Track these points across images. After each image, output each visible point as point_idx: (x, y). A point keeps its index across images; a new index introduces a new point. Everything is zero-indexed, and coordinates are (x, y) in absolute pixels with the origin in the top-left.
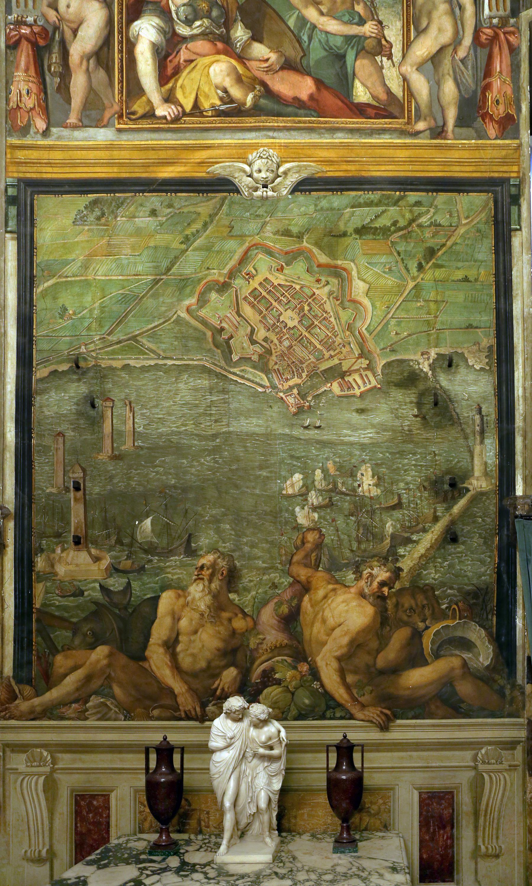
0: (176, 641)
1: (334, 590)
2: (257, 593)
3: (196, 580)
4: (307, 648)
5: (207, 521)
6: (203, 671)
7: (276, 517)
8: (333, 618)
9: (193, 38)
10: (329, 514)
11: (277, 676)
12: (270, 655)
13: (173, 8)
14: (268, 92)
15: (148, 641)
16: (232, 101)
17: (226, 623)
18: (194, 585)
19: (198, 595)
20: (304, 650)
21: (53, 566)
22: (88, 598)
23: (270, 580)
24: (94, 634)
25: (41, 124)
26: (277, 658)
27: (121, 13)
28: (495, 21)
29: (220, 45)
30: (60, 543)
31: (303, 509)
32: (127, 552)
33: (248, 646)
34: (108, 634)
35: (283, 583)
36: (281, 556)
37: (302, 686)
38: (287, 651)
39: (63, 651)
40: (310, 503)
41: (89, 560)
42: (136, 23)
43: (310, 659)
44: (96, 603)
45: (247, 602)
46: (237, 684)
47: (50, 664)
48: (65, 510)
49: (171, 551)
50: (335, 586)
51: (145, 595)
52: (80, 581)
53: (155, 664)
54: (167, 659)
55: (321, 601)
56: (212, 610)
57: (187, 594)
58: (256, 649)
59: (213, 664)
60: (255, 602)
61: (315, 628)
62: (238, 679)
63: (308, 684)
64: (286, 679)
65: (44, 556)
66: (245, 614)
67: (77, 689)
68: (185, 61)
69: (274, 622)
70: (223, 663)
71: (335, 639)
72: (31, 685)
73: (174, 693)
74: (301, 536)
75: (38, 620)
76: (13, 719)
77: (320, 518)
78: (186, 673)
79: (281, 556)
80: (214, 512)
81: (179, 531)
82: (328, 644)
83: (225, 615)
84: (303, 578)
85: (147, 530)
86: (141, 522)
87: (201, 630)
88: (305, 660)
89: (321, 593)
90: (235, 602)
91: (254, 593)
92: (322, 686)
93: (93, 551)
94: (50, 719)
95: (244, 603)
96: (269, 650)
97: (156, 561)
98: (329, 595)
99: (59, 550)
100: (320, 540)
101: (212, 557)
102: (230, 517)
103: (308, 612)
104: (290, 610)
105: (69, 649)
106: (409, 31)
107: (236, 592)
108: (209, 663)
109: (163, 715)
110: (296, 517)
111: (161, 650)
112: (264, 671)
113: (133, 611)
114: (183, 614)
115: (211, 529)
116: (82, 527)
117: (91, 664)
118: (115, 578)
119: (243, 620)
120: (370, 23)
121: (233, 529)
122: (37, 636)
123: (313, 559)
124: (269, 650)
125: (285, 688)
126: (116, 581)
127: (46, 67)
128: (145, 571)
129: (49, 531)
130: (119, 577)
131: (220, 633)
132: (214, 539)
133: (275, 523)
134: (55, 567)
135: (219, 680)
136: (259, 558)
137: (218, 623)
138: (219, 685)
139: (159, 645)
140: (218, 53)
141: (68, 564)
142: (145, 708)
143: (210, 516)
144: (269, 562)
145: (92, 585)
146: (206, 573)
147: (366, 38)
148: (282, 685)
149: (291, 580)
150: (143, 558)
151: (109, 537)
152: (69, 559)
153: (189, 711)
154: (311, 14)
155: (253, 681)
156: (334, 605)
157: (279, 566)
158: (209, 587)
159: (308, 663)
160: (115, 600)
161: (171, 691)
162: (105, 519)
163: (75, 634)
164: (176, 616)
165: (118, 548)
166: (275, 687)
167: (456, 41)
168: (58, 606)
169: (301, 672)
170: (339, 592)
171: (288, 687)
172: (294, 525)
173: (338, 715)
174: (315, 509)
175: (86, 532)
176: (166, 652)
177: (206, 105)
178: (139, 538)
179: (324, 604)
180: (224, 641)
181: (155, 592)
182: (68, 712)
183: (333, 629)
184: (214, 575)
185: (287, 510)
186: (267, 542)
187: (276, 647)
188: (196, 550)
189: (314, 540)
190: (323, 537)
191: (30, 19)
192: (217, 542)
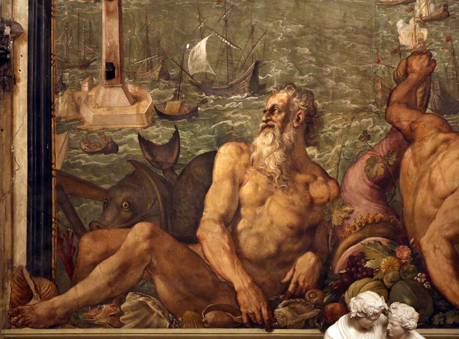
0: (238, 216)
1: (446, 141)
2: (343, 146)
3: (263, 128)
4: (408, 225)
5: (280, 42)
6: (272, 257)
7: (370, 36)
8: (444, 181)
10: (443, 29)
11: (368, 264)
12: (359, 235)
15: (201, 216)
17: (301, 188)
18: (262, 134)
19: (266, 150)
20: (405, 228)
21: (77, 109)
22: (124, 155)
23: (361, 127)
24: (131, 206)
26: (368, 239)
30: (87, 76)
31: (408, 23)
32: (174, 89)
33: (330, 221)
34: (149, 206)
35: (378, 131)
36: (376, 92)
37: (402, 279)
38: (381, 230)
39: (91, 230)
40: (417, 15)
41: (124, 100)
43: (412, 241)
44: (133, 162)
45: (330, 160)
46: (316, 277)
47: (75, 248)
48: (94, 28)
49: (232, 86)
50: (448, 136)
51: (198, 150)
52: (113, 131)
53: (209, 249)
54: (225, 241)
55: (429, 157)
56: (284, 170)
57: (251, 149)
58: (341, 227)
59: (284, 248)
60: (340, 160)
61: (419, 196)
62: (317, 268)
63: (409, 276)
64: (380, 268)
65: (66, 95)
66: (327, 177)
67: (110, 284)
69: (364, 187)
70: (296, 247)
71: (446, 212)
72: (51, 279)
73: (233, 288)
74: (403, 63)
75: (59, 187)
77: (430, 35)
78: (250, 261)
79: (376, 92)
80: (289, 30)
81: (243, 58)
82: (437, 219)
83: (301, 178)
84: (405, 124)
85: (201, 57)
86: (193, 44)
87: (269, 200)
88: (406, 242)
89: (428, 145)
90: (313, 160)
91: (339, 146)
92: (429, 278)
93: (131, 88)
94: (75, 326)
95: (326, 161)
96: (358, 228)
97: (212, 101)
98: (439, 149)
99: (86, 87)
100: (430, 69)
101: (285, 94)
102: (310, 37)
103: (410, 173)
104: (386, 171)
105: (98, 228)
107: (316, 145)
108: (279, 245)
109: (219, 320)
110: (398, 35)
111: (217, 228)
112: (351, 258)
113: (182, 174)
114: (247, 177)
115: (284, 55)
116: (115, 52)
117: (127, 248)
118: (158, 127)
119: (324, 186)
121: (313, 55)
122: (57, 211)
123: (419, 96)
124: (358, 228)
125: (379, 282)
126: (160, 130)
128: (197, 116)
129: (73, 58)
130: (164, 124)
131: (293, 203)
132: (289, 69)
133: (369, 45)
134: (81, 111)
135: (292, 271)
136: (346, 96)
137: (291, 190)
138: (292, 277)
139: (215, 221)
141: (98, 106)
142: (195, 311)
143: (283, 36)
144: (360, 100)
145: (129, 136)
146: (278, 117)
148: (375, 278)
149: (389, 127)
150: (195, 98)
151: (151, 68)
152: (99, 100)
153: (253, 313)
155: (336, 272)
156: (445, 162)
157: (374, 107)
158: (281, 138)
159: (410, 246)
160: (159, 158)
161: (229, 286)
162: (146, 41)
163: (106, 205)
164: (238, 181)
165: (163, 83)
166: (365, 280)
168: (84, 167)
169: (400, 259)
170: (453, 144)
171: (382, 281)
172: (395, 47)
173: (450, 321)
174: (423, 22)
175: (122, 60)
176: (224, 232)
178: (190, 68)
179: (432, 162)
180: (300, 215)
181: (210, 145)
182: (98, 316)
183: (444, 198)
184: (288, 121)
185: (386, 26)
186: (359, 72)
187: (367, 223)
188: (264, 86)
189: (421, 69)
190: (433, 64)
192: (292, 73)
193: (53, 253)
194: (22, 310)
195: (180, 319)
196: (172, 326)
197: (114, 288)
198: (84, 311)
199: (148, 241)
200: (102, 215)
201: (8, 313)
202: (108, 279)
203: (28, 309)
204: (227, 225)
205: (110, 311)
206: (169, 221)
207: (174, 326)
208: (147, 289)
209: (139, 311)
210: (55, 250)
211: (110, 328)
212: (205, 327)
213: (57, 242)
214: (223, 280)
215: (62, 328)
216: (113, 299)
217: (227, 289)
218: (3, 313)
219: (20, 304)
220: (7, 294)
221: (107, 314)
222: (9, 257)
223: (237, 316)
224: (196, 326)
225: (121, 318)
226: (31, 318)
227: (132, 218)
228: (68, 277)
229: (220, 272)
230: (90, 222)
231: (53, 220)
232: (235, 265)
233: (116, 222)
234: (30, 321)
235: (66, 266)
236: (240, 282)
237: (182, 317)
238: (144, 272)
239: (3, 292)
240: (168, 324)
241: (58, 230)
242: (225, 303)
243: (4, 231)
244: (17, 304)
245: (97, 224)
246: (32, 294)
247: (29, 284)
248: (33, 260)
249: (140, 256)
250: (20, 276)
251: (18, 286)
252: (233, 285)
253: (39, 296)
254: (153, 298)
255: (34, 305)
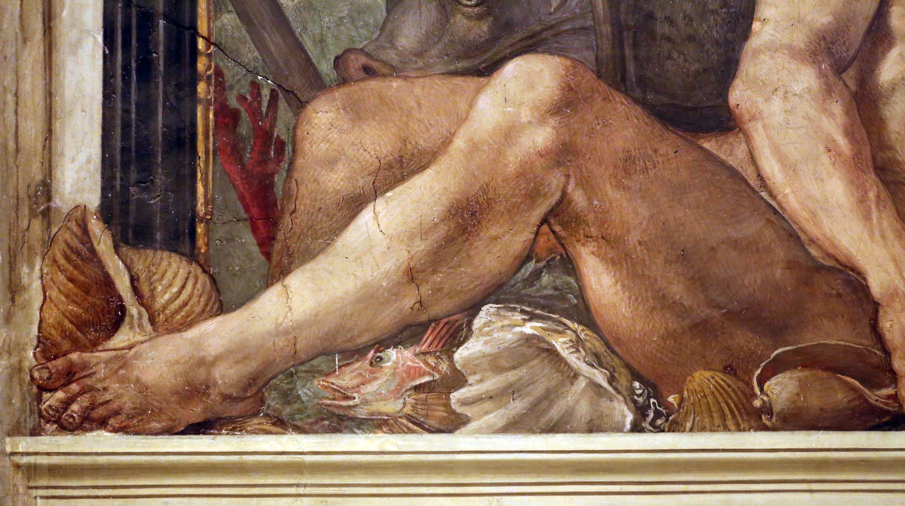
15: (746, 34)
39: (344, 81)
47: (281, 145)
53: (777, 151)
67: (412, 275)
72: (192, 256)
76: (102, 424)
94: (281, 424)
105: (369, 72)
109: (814, 401)
139: (795, 53)
142: (729, 369)
176: (828, 90)
193: (201, 163)
194: (85, 366)
195: (671, 399)
196: (646, 425)
197: (425, 290)
198: (314, 373)
199: (553, 121)
200: (382, 29)
201: (32, 378)
202: (404, 255)
203: (108, 362)
204: (840, 69)
205: (412, 373)
206: (628, 52)
207: (652, 424)
208: (550, 292)
209: (522, 372)
210: (207, 152)
211: (413, 432)
212: (765, 428)
213: (216, 122)
214: (830, 263)
215: (233, 431)
216: (425, 326)
217: (841, 291)
218: (11, 378)
219: (77, 346)
220: (25, 306)
221: (403, 380)
222: (36, 173)
223: (880, 386)
224: (730, 423)
225: (455, 396)
226: (119, 396)
227: (494, 39)
228: (255, 249)
229: (814, 231)
230: (340, 52)
231: (201, 44)
232: (870, 207)
233: (434, 52)
234: (115, 406)
235: (247, 208)
236: (891, 267)
237: (681, 392)
238: (537, 233)
239: (13, 300)
240: (630, 418)
241: (218, 78)
242: (834, 342)
243: (18, 79)
244: (66, 345)
245: (363, 60)
246: (123, 309)
247: (111, 272)
248: (125, 188)
249: (521, 174)
250: (75, 243)
251: (71, 280)
252: (865, 279)
253: (146, 316)
254: (575, 326)
255: (130, 348)
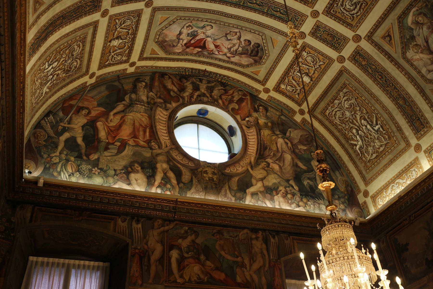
9: (189, 258)
13: (183, 248)
14: (211, 277)
16: (201, 279)
25: (140, 282)
27: (167, 248)
28: (274, 260)
29: (197, 261)
42: (172, 251)
68: (187, 265)
106: (251, 261)
120: (240, 257)
127: (143, 263)
140: (196, 263)
147: (239, 262)
154: (223, 253)
167: (264, 265)
177: (193, 279)
191: (139, 248)
